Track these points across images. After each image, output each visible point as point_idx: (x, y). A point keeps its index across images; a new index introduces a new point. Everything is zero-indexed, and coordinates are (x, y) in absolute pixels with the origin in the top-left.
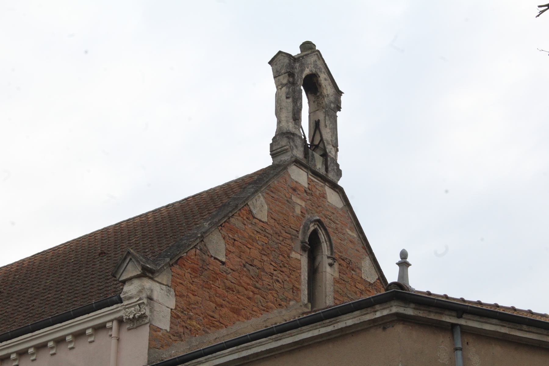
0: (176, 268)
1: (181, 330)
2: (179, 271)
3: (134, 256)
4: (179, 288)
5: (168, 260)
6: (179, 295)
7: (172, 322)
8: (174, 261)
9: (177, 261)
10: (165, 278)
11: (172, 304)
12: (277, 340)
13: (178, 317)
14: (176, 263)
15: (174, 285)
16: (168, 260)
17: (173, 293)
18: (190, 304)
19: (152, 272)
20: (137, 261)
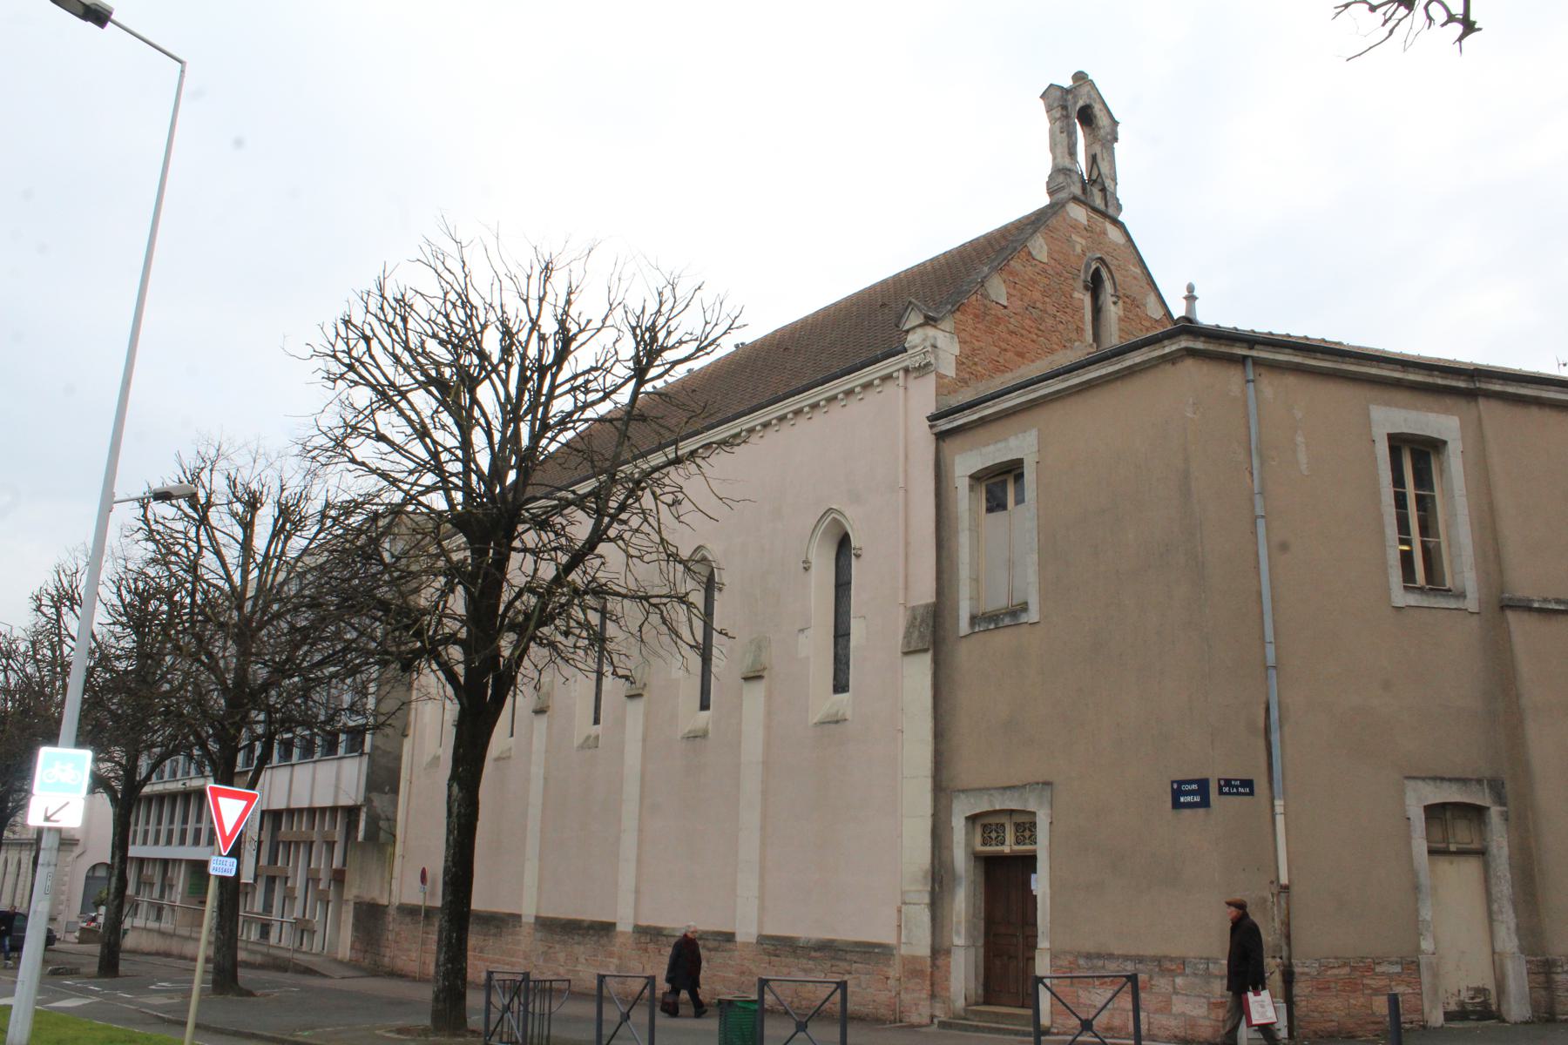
0: (958, 315)
1: (967, 376)
2: (962, 317)
3: (915, 305)
4: (963, 335)
5: (949, 307)
6: (962, 342)
7: (957, 369)
8: (956, 307)
9: (958, 308)
10: (947, 324)
11: (956, 350)
12: (1078, 376)
13: (963, 363)
14: (958, 310)
15: (957, 332)
16: (949, 307)
17: (956, 339)
18: (974, 350)
19: (934, 320)
20: (920, 311)
